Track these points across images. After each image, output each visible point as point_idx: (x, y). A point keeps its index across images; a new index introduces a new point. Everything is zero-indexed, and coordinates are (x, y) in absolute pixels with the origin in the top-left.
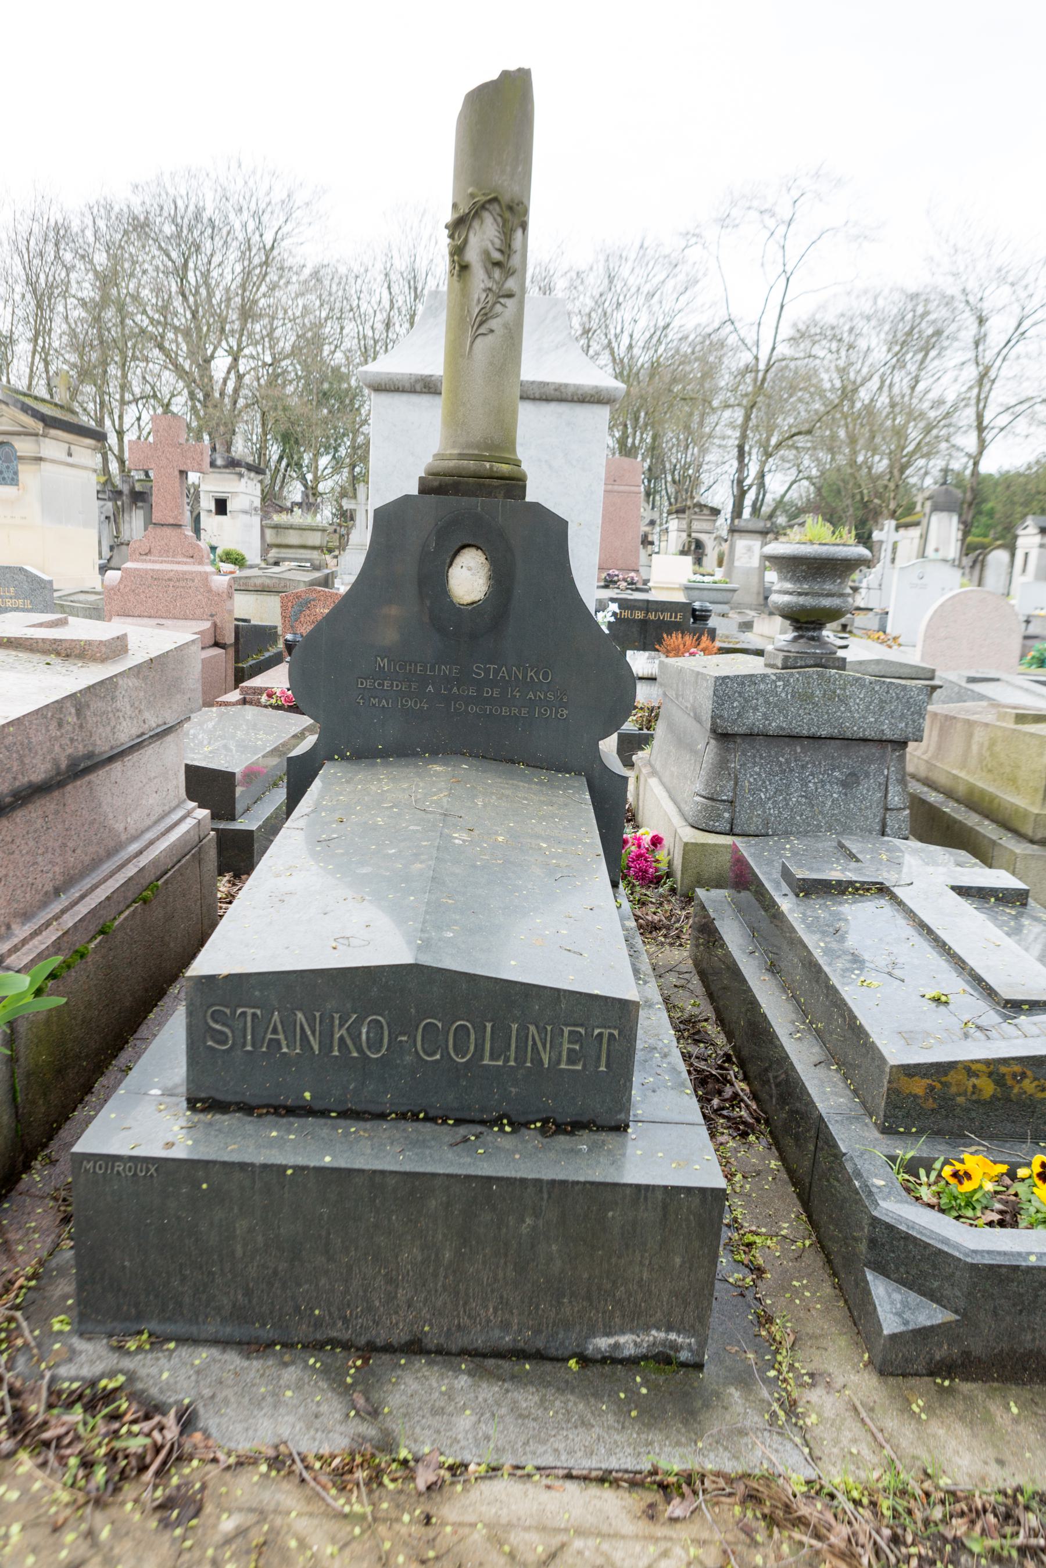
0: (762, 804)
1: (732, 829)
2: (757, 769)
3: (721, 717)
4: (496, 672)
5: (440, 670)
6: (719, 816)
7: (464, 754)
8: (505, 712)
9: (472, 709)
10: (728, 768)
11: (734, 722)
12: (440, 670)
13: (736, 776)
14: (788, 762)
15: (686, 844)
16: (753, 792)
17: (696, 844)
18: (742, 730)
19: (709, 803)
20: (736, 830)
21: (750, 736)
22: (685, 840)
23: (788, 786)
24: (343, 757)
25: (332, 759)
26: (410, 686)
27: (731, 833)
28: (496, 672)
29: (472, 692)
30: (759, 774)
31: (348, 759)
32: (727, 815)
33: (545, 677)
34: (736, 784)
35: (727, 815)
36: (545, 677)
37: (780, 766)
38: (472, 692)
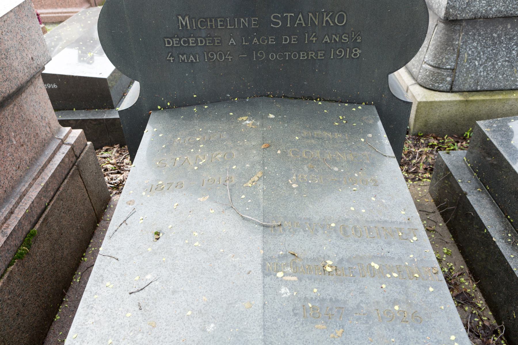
0: (476, 68)
1: (451, 88)
2: (475, 44)
3: (454, 7)
4: (293, 20)
5: (239, 22)
6: (443, 80)
7: (268, 96)
8: (303, 56)
9: (273, 57)
10: (452, 45)
11: (463, 10)
12: (239, 22)
13: (459, 51)
14: (499, 36)
15: (419, 103)
16: (469, 61)
17: (426, 102)
18: (468, 16)
19: (436, 70)
20: (455, 89)
21: (473, 20)
22: (419, 99)
23: (496, 55)
24: (165, 107)
25: (156, 109)
26: (213, 41)
27: (451, 91)
28: (293, 20)
29: (271, 41)
30: (476, 48)
31: (169, 108)
32: (449, 79)
33: (340, 21)
34: (458, 56)
35: (449, 79)
36: (340, 21)
37: (493, 40)
38: (271, 41)
